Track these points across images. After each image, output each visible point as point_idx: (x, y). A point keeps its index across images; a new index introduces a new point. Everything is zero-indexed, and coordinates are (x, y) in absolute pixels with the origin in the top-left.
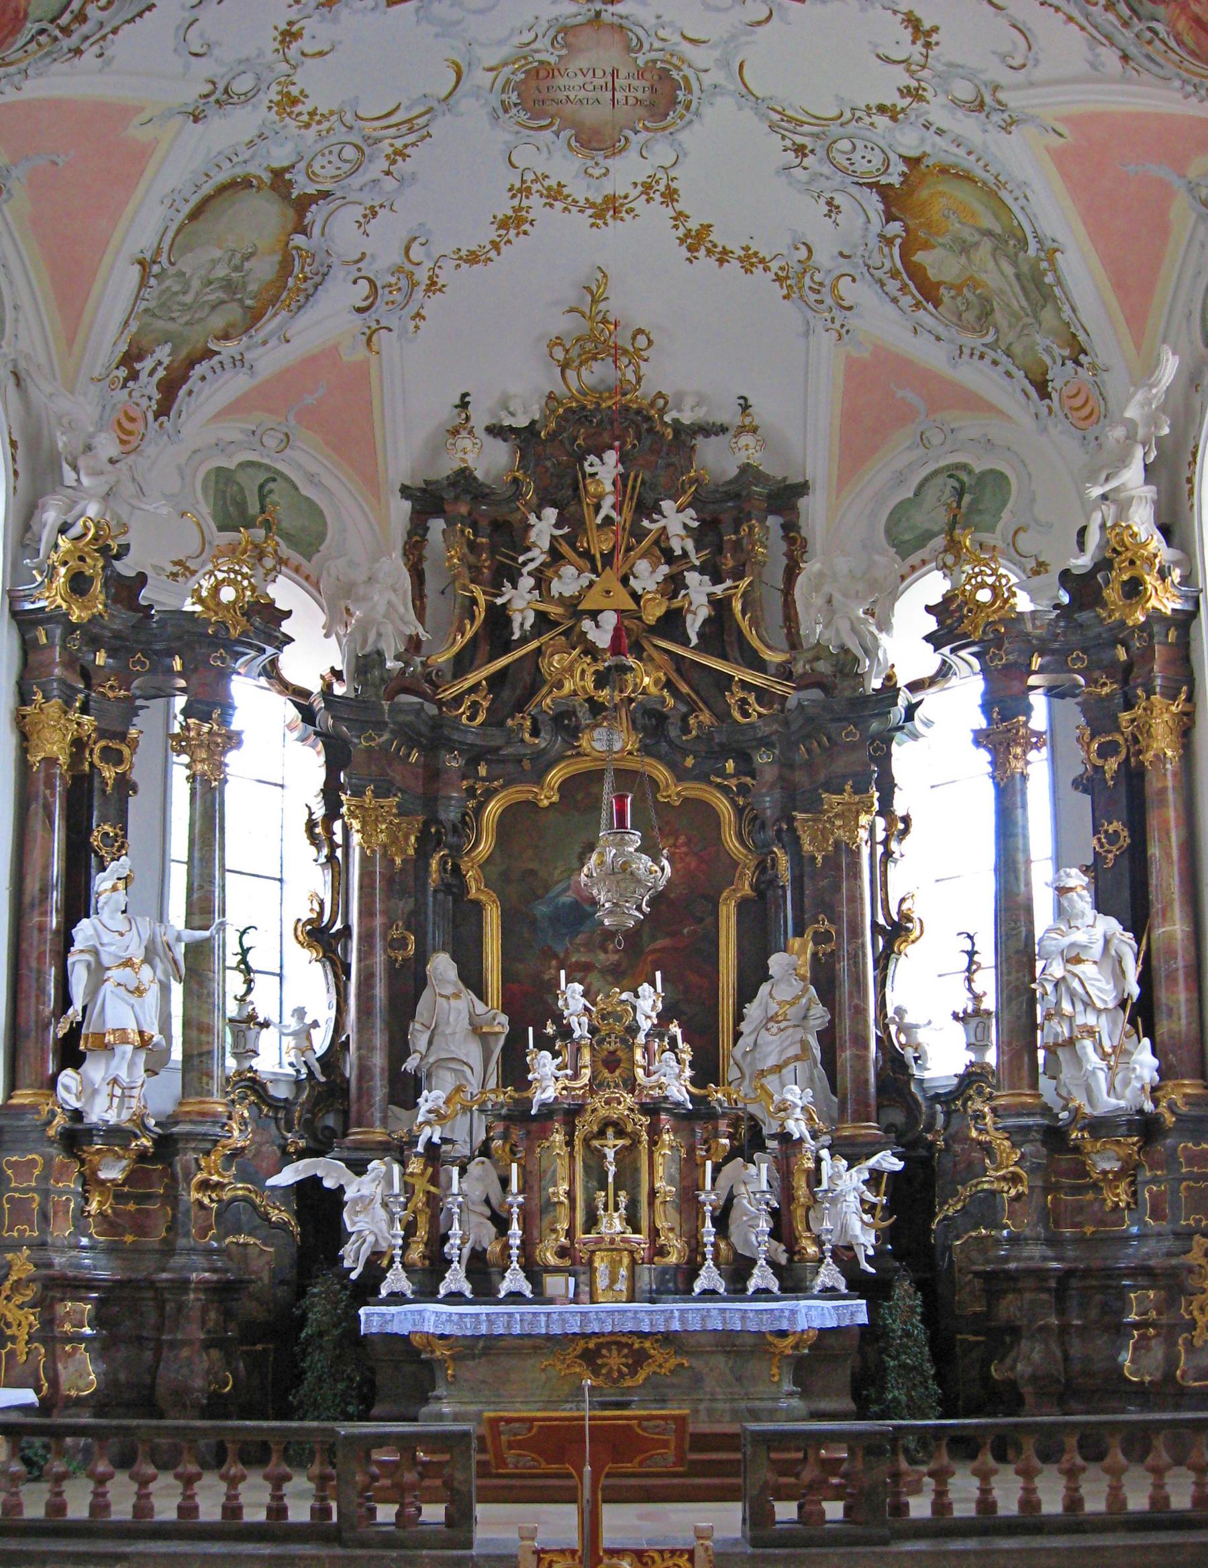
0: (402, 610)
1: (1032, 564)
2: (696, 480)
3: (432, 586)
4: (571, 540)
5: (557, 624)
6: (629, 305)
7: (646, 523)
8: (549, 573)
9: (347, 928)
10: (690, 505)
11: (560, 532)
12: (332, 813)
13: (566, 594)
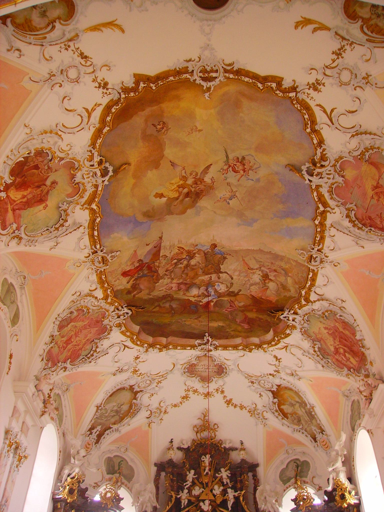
0: (153, 499)
1: (317, 487)
2: (230, 463)
3: (161, 491)
4: (198, 479)
5: (193, 503)
6: (214, 418)
7: (217, 475)
8: (192, 488)
10: (228, 469)
11: (195, 477)
13: (196, 494)
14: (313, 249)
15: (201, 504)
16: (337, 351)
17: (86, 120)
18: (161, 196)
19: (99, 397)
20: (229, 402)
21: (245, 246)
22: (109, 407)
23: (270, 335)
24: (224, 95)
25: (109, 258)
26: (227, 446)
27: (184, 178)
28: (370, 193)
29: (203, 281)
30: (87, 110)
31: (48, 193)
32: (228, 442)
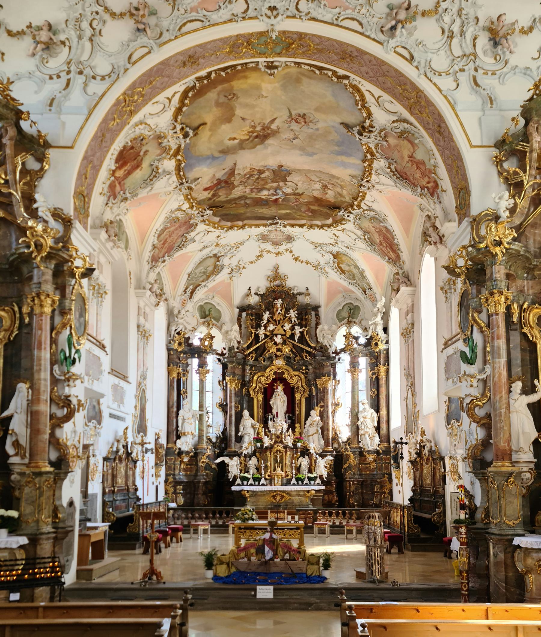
4: (272, 318)
9: (227, 404)
12: (224, 379)
14: (362, 180)
15: (275, 338)
16: (381, 244)
17: (167, 105)
18: (234, 139)
19: (190, 268)
20: (296, 259)
21: (306, 167)
22: (197, 271)
23: (330, 221)
24: (286, 74)
25: (193, 186)
26: (295, 292)
27: (254, 127)
28: (407, 159)
29: (272, 186)
30: (168, 98)
31: (142, 160)
32: (296, 288)
